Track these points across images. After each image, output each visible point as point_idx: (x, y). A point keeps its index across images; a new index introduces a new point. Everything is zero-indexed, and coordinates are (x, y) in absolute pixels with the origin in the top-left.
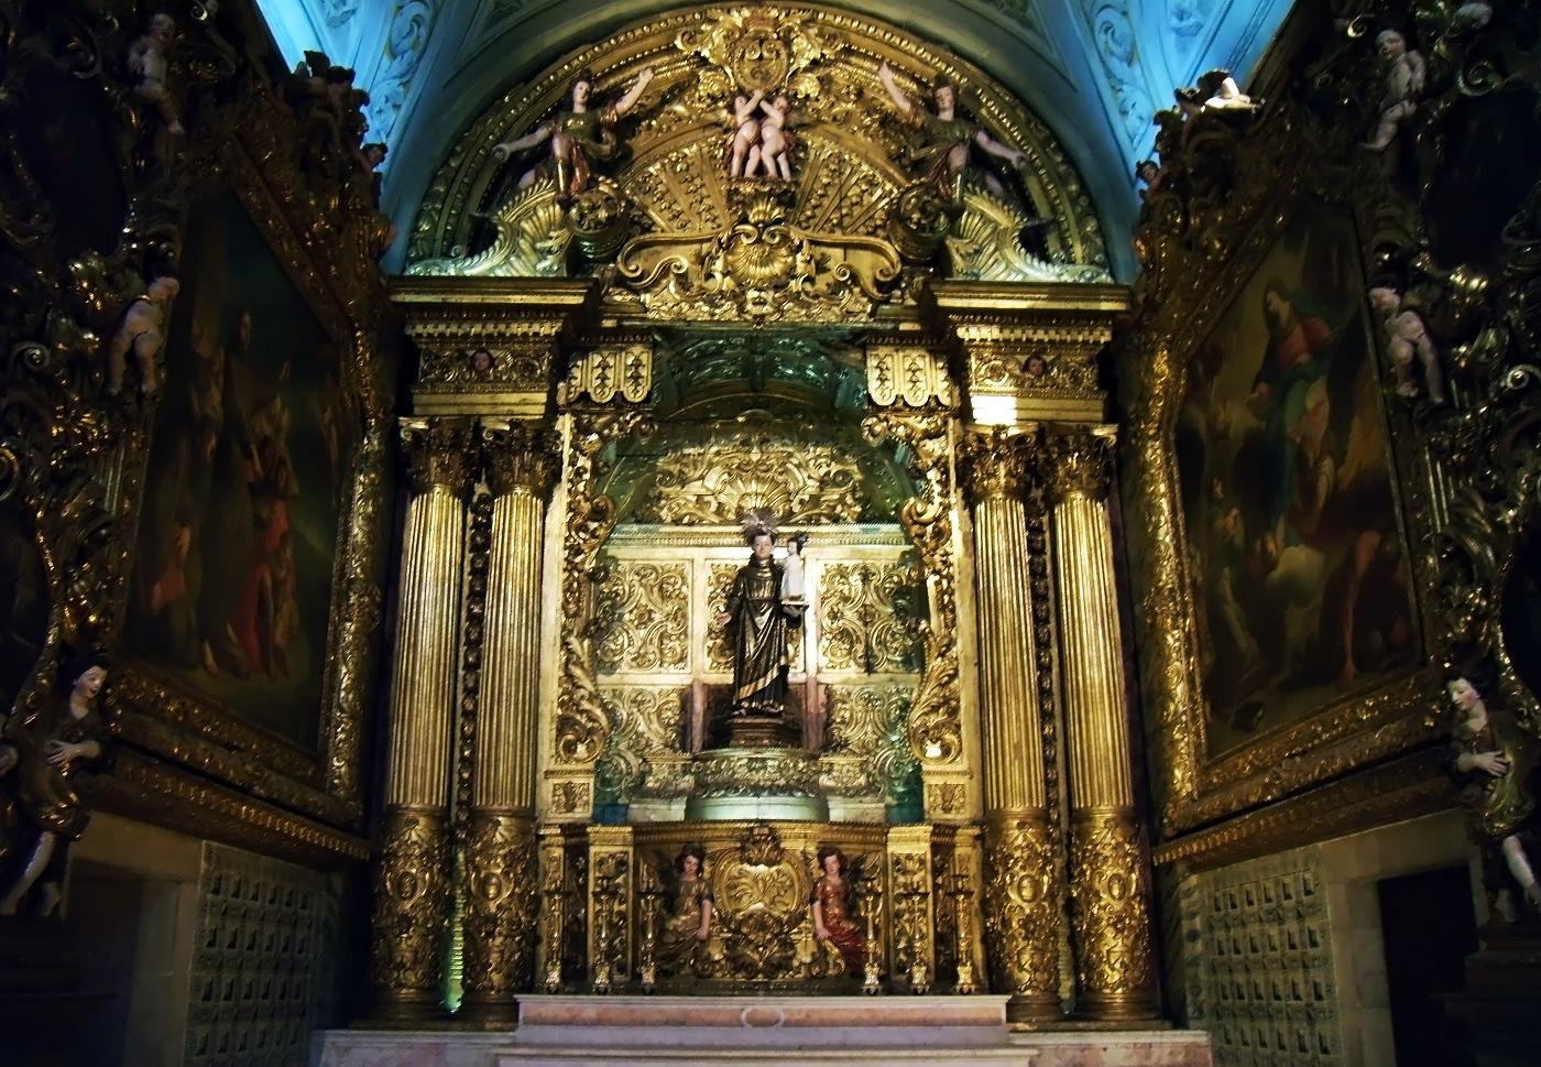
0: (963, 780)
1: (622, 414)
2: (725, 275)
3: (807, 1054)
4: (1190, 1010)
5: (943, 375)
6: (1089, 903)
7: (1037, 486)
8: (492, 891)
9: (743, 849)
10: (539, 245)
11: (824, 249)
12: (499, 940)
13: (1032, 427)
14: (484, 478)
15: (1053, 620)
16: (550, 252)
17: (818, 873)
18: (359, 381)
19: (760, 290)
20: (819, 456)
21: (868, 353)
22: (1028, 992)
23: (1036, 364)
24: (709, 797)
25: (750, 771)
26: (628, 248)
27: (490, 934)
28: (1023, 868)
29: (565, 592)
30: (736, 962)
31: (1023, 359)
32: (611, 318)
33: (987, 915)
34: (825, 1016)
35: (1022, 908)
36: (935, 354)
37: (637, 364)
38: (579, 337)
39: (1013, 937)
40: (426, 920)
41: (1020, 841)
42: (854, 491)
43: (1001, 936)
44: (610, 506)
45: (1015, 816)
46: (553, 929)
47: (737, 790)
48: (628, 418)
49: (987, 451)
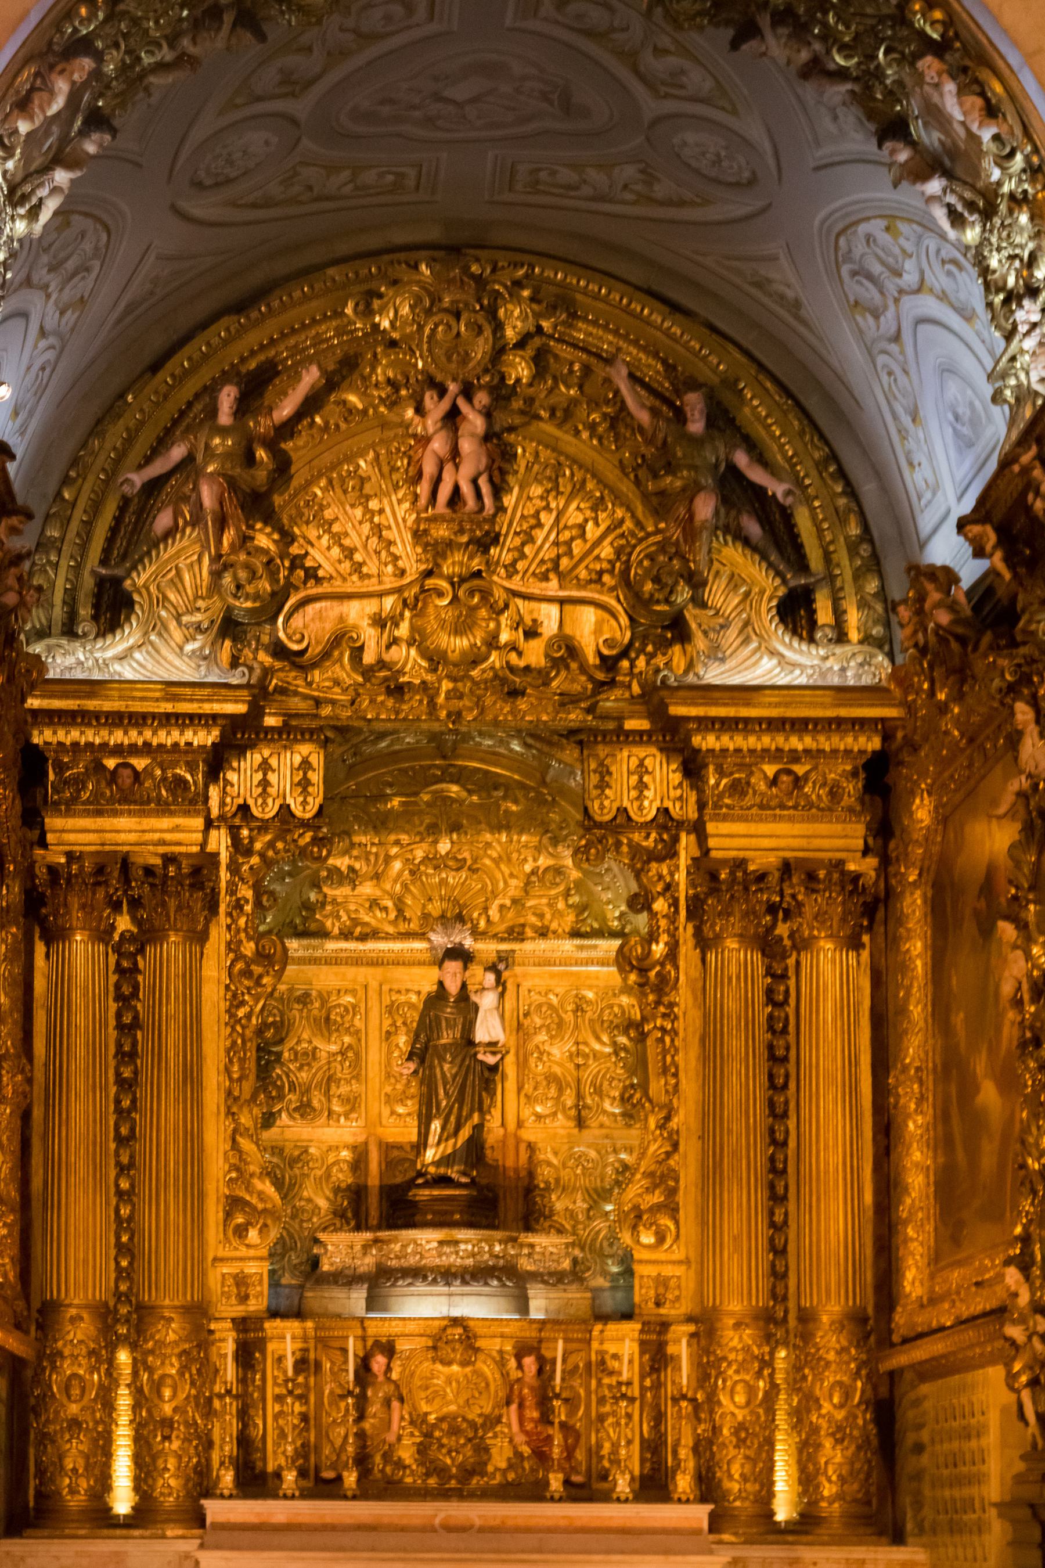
0: (679, 1271)
8: (167, 1393)
9: (435, 1348)
12: (176, 1445)
24: (393, 1285)
27: (167, 1438)
29: (228, 1051)
34: (521, 1522)
37: (306, 765)
39: (724, 1445)
42: (567, 894)
43: (711, 1443)
45: (732, 1314)
47: (425, 1278)
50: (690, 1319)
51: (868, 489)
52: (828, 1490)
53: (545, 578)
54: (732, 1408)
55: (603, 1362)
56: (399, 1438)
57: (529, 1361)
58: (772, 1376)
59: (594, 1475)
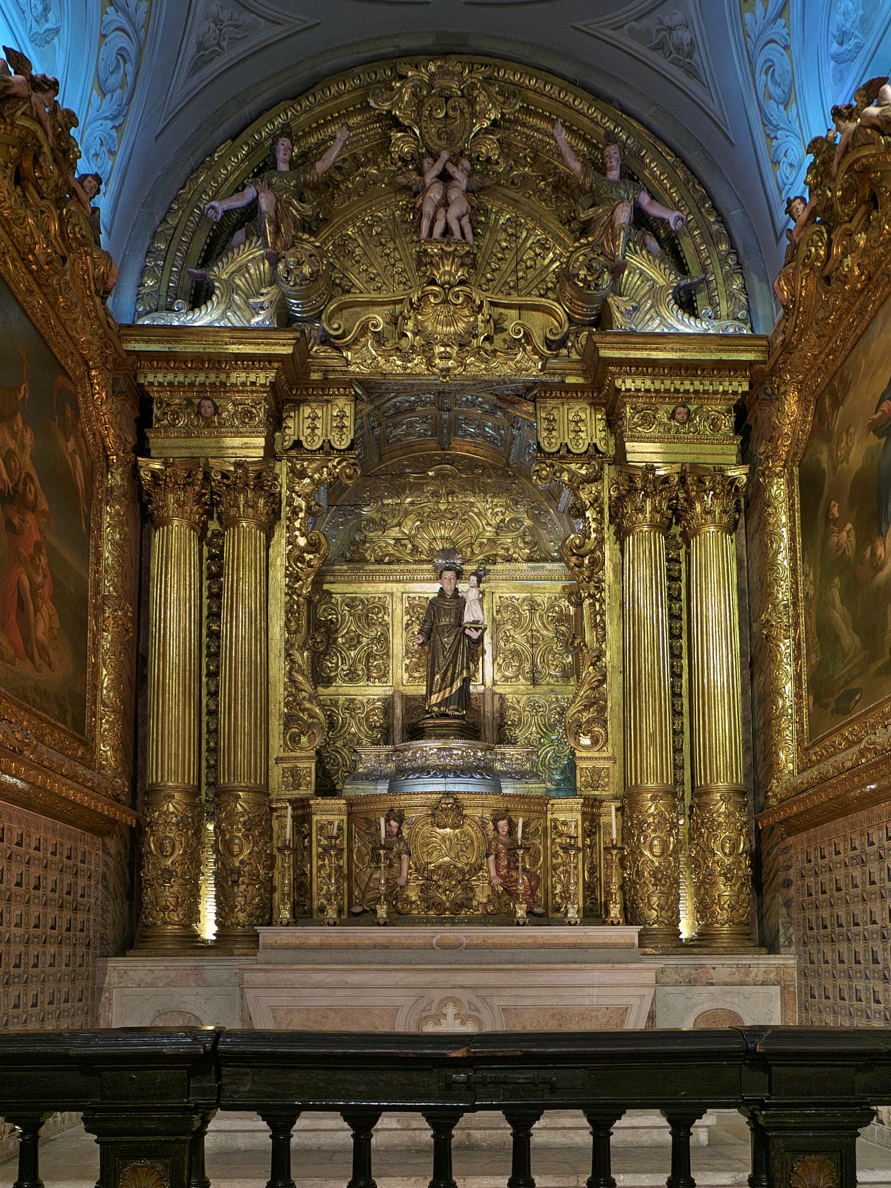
0: (607, 764)
1: (330, 460)
2: (415, 334)
6: (705, 858)
7: (677, 524)
11: (502, 310)
13: (677, 468)
14: (215, 516)
15: (684, 635)
16: (263, 309)
19: (445, 345)
20: (496, 505)
21: (538, 405)
22: (656, 926)
28: (654, 831)
29: (287, 612)
31: (671, 408)
32: (318, 371)
33: (624, 868)
35: (653, 862)
36: (595, 405)
38: (291, 389)
41: (652, 810)
44: (323, 540)
46: (284, 880)
47: (429, 773)
48: (335, 464)
49: (636, 490)
50: (616, 798)
51: (735, 215)
59: (550, 908)
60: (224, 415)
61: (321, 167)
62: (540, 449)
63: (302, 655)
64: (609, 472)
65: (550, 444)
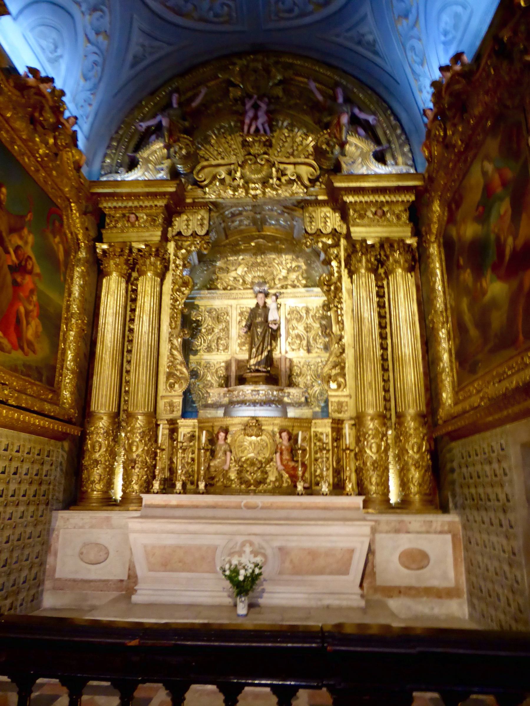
0: (346, 399)
3: (267, 522)
4: (451, 505)
5: (338, 219)
8: (134, 449)
10: (157, 167)
11: (286, 166)
12: (137, 470)
16: (162, 170)
17: (278, 440)
18: (74, 226)
23: (380, 212)
25: (252, 395)
26: (199, 167)
27: (133, 467)
30: (242, 480)
36: (334, 210)
37: (202, 219)
38: (176, 208)
39: (368, 470)
40: (106, 461)
43: (362, 469)
45: (369, 415)
47: (246, 404)
52: (414, 489)
53: (288, 157)
54: (371, 454)
55: (316, 435)
56: (230, 468)
57: (284, 434)
58: (387, 440)
60: (141, 221)
61: (194, 104)
62: (306, 232)
63: (177, 340)
64: (343, 242)
65: (311, 229)
